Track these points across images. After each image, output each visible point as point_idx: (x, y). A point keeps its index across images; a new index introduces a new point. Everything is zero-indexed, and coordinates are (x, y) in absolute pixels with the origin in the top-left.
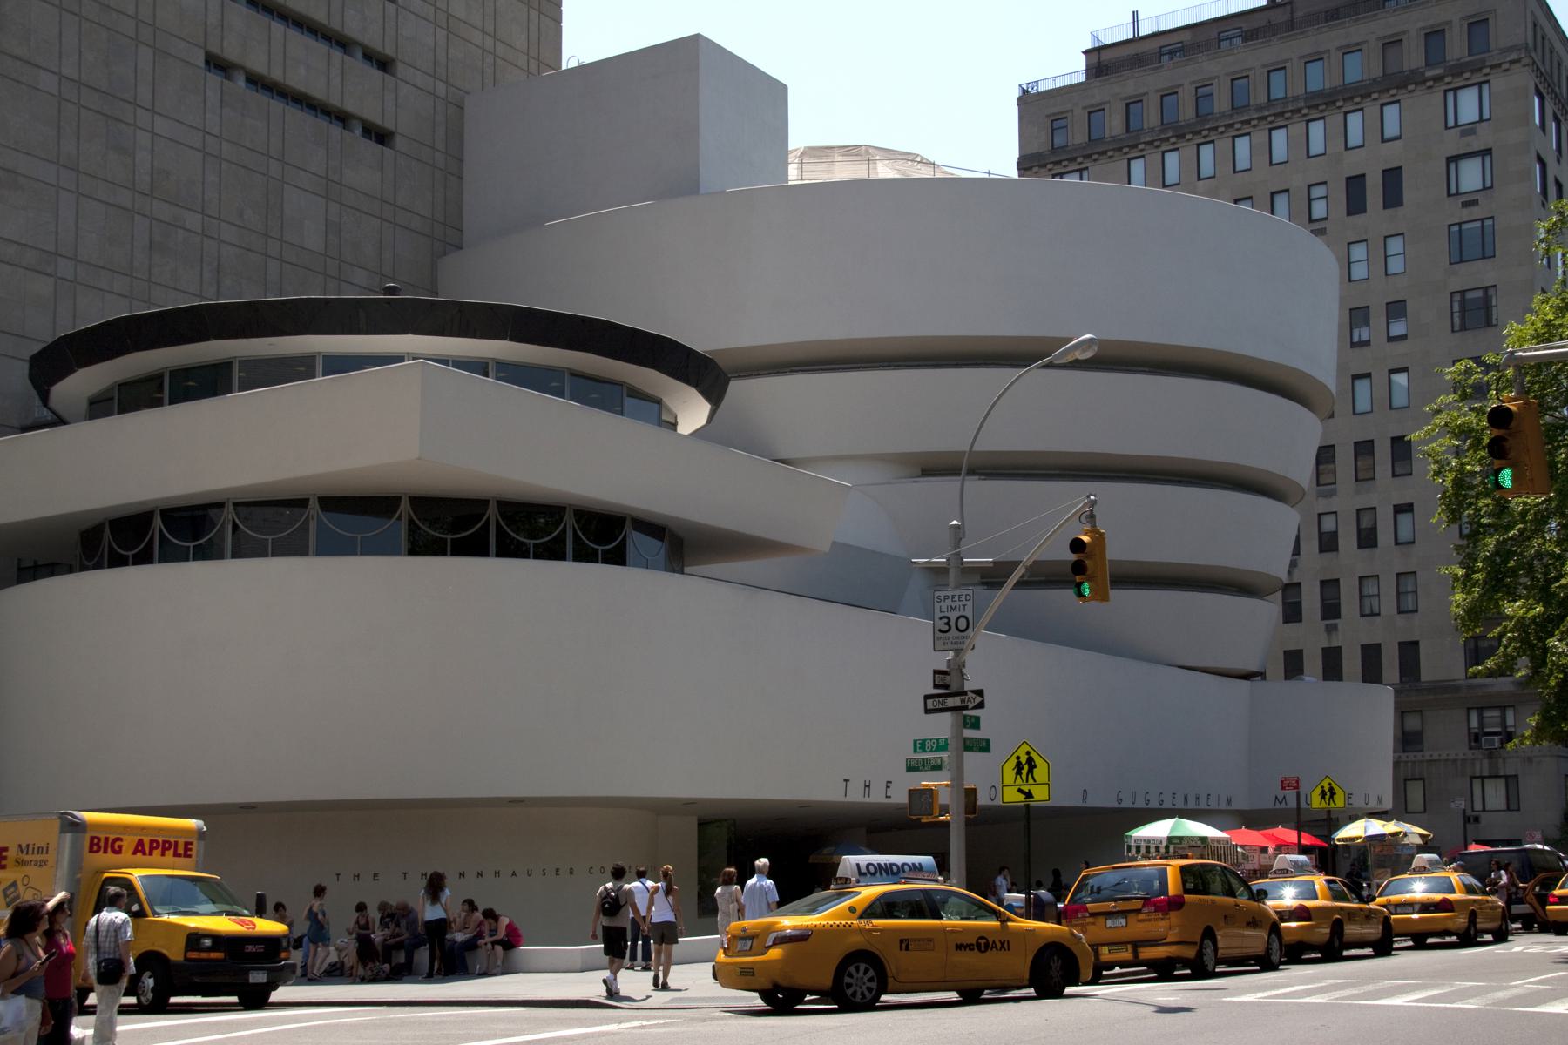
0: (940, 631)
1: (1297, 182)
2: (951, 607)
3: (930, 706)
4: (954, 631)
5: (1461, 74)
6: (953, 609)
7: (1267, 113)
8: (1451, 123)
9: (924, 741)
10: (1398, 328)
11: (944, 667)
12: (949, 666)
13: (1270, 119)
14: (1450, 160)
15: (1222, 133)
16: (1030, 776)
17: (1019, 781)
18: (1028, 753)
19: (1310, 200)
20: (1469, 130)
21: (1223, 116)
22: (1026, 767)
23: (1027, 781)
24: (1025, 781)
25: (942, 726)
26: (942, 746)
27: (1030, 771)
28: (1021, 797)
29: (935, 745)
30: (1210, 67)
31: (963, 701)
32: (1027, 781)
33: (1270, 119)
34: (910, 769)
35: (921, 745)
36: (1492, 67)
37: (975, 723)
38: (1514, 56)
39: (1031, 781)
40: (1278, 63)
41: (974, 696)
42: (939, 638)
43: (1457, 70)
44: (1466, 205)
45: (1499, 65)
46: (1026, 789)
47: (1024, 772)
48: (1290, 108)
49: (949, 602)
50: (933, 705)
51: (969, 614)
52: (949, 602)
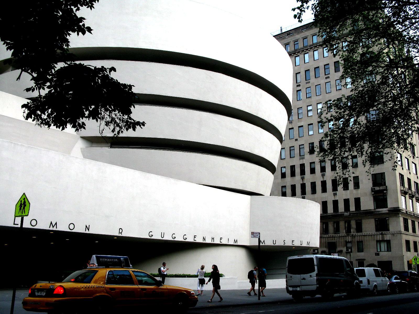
1: (321, 65)
7: (312, 47)
13: (313, 48)
15: (301, 53)
19: (325, 69)
21: (301, 49)
30: (298, 36)
33: (313, 48)
40: (315, 34)
48: (318, 45)
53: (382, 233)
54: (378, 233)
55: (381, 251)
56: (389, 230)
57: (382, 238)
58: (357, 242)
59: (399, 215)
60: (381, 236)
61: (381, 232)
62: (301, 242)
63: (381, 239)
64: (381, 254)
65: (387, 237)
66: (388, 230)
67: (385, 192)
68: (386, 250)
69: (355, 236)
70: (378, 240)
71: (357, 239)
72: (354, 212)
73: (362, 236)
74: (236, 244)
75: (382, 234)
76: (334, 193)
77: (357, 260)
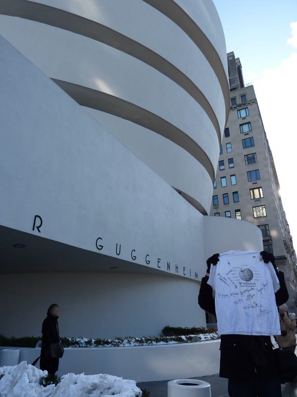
5: (241, 106)
8: (239, 117)
10: (231, 165)
14: (240, 125)
20: (244, 118)
36: (248, 104)
38: (253, 101)
43: (240, 105)
44: (245, 135)
45: (249, 104)
67: (270, 241)
74: (196, 279)
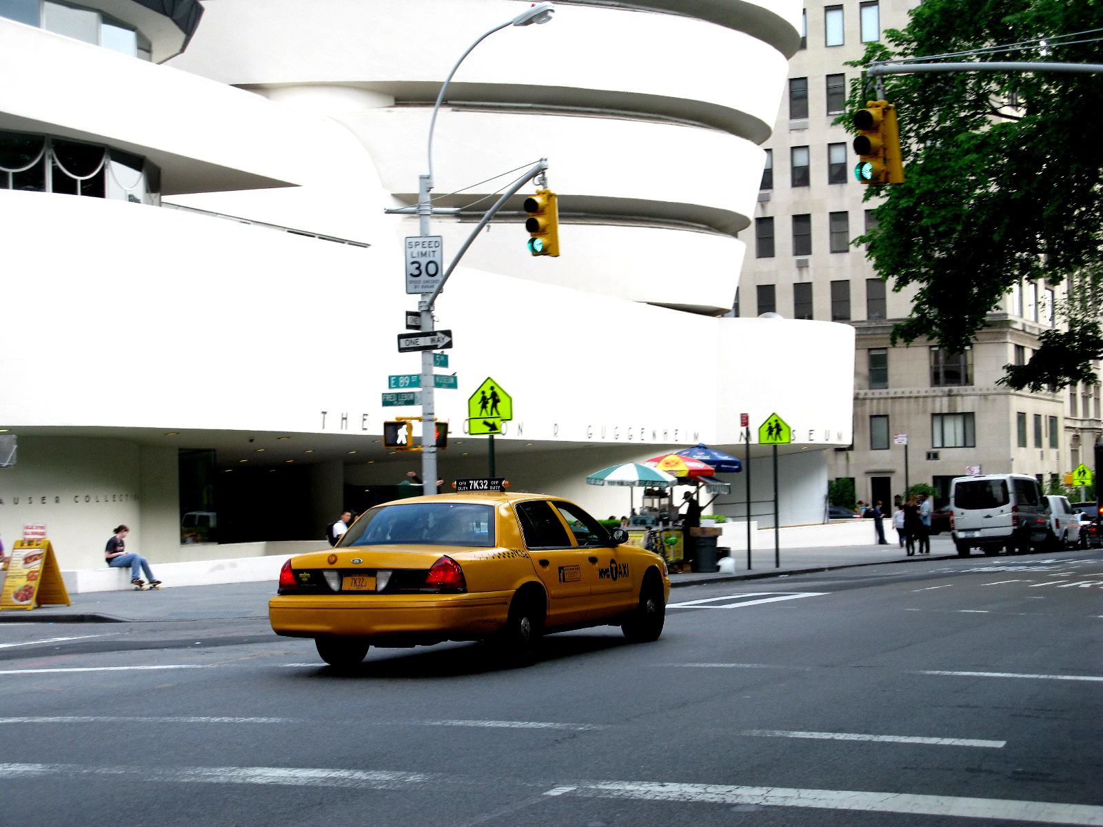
0: (412, 275)
2: (422, 253)
3: (403, 345)
4: (424, 276)
6: (424, 255)
9: (398, 377)
11: (416, 309)
12: (420, 307)
16: (494, 410)
17: (484, 414)
18: (492, 388)
22: (491, 402)
23: (492, 414)
24: (489, 412)
25: (413, 363)
26: (415, 381)
27: (494, 405)
28: (487, 429)
29: (408, 382)
31: (433, 340)
32: (492, 414)
34: (386, 403)
35: (395, 381)
37: (444, 362)
39: (495, 414)
41: (443, 336)
42: (411, 282)
46: (490, 421)
47: (489, 405)
49: (419, 249)
50: (406, 343)
51: (437, 259)
52: (419, 249)
53: (950, 391)
54: (939, 390)
55: (943, 447)
56: (972, 385)
57: (950, 406)
58: (872, 417)
59: (1005, 338)
60: (945, 400)
61: (946, 389)
62: (827, 433)
63: (945, 411)
64: (943, 453)
65: (964, 405)
66: (968, 381)
68: (960, 443)
69: (864, 399)
70: (937, 411)
71: (871, 407)
72: (864, 325)
73: (886, 399)
75: (950, 395)
76: (799, 262)
77: (868, 473)
